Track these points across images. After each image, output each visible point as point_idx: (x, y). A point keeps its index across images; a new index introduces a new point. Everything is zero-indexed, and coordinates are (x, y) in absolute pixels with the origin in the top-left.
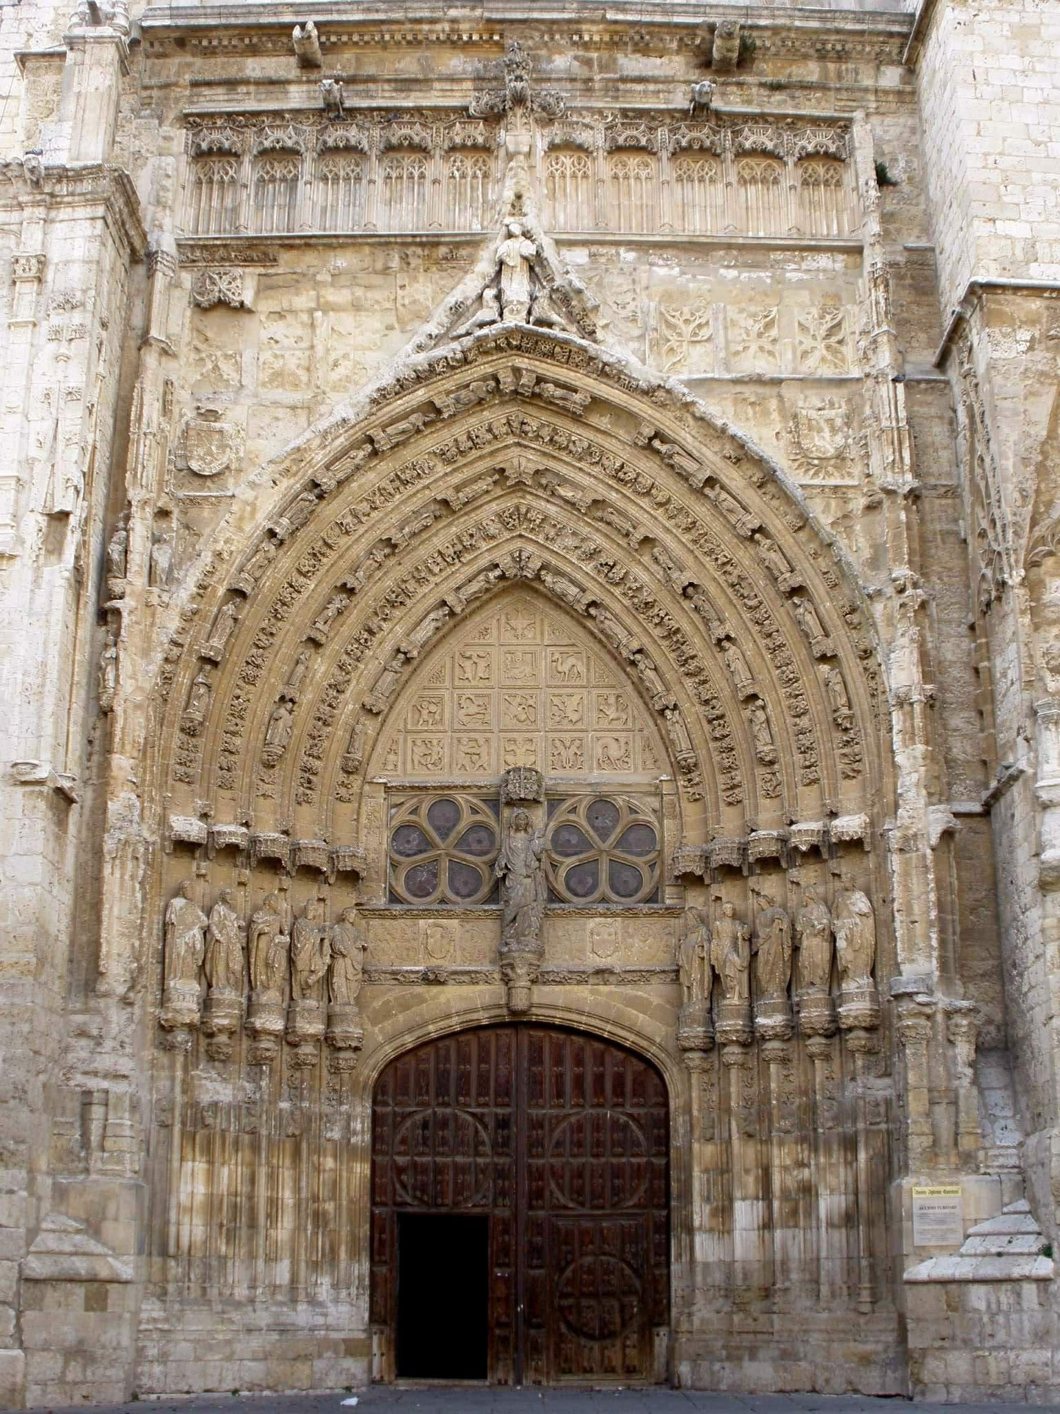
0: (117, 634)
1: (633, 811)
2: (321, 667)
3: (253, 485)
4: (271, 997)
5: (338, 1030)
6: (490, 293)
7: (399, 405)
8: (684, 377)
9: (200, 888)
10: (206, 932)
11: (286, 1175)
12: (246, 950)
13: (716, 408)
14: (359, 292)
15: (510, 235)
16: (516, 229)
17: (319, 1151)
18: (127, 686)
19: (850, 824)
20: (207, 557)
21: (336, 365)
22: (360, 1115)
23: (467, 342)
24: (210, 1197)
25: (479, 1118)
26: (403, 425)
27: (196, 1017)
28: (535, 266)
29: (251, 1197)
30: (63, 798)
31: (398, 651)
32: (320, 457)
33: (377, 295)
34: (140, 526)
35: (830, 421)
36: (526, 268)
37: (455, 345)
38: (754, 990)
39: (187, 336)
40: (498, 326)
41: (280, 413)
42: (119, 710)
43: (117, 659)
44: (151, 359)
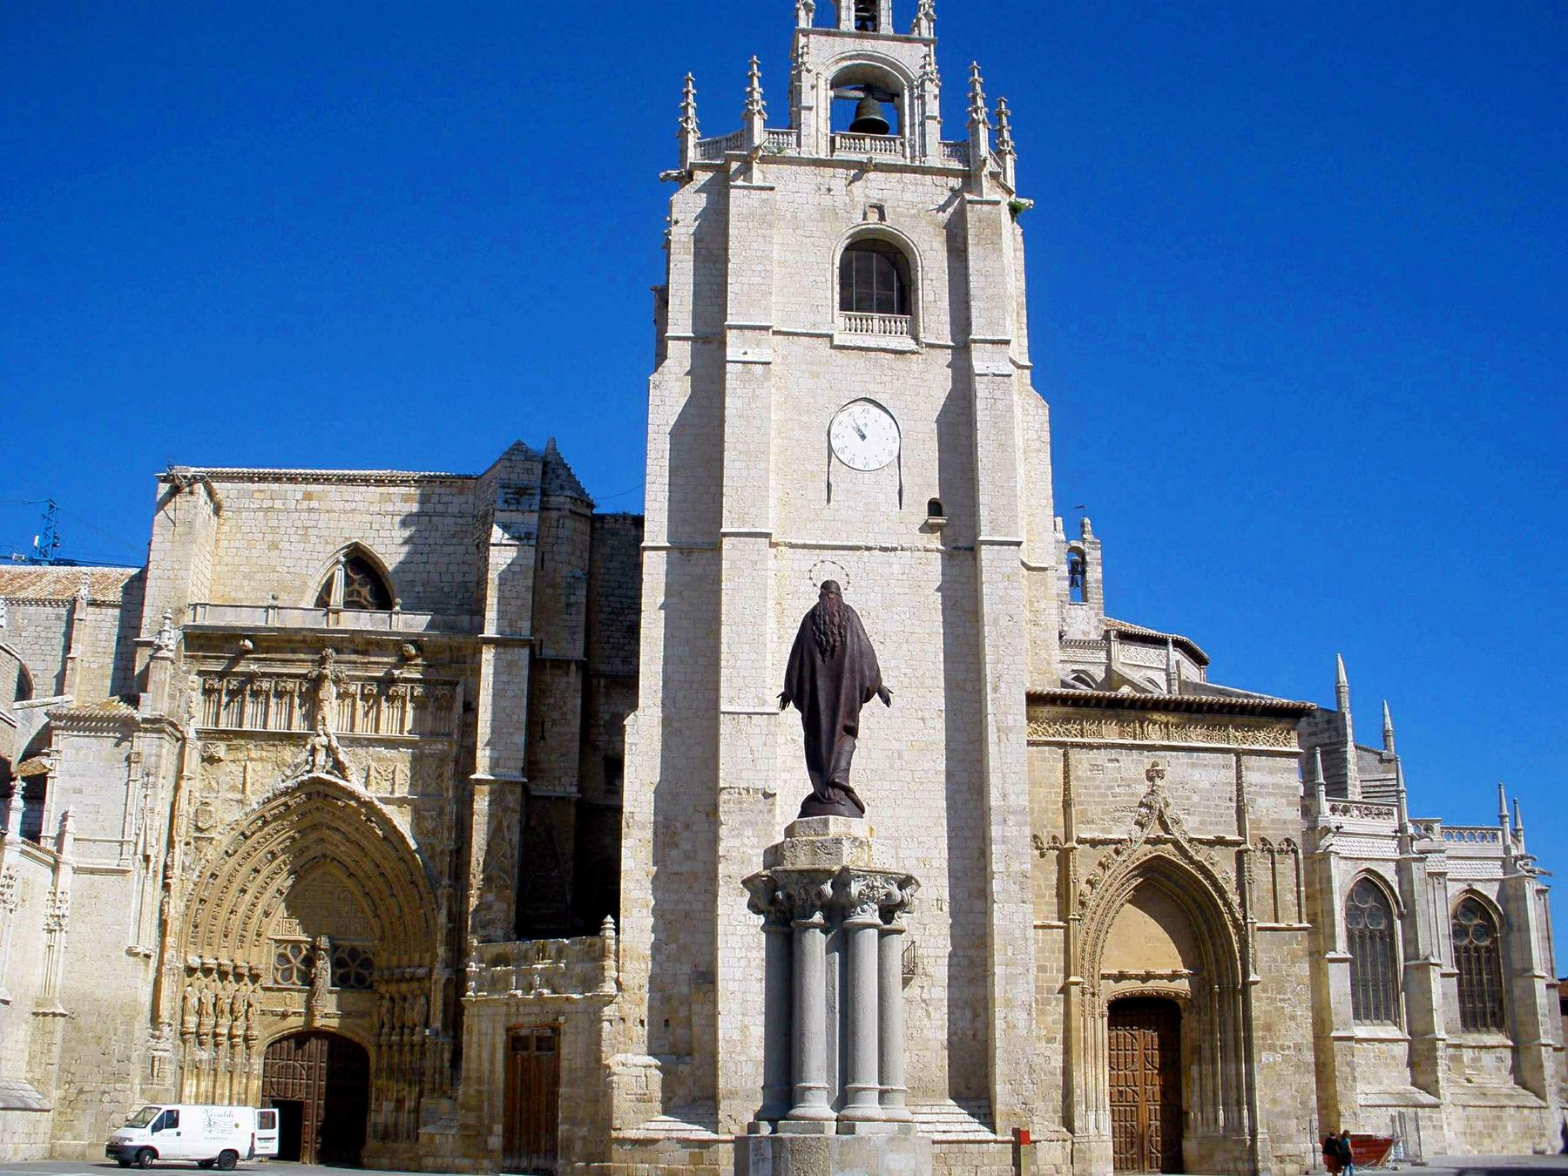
0: (168, 891)
1: (365, 952)
2: (248, 897)
3: (220, 833)
4: (225, 1021)
5: (249, 1033)
6: (311, 758)
7: (274, 804)
8: (379, 795)
9: (198, 982)
10: (200, 999)
11: (227, 1084)
12: (215, 1005)
13: (389, 811)
14: (264, 753)
15: (319, 736)
16: (321, 733)
17: (241, 1076)
18: (172, 911)
19: (421, 972)
20: (203, 862)
21: (253, 784)
22: (257, 1064)
23: (299, 779)
24: (197, 1092)
25: (302, 1066)
26: (276, 811)
27: (194, 1030)
28: (330, 750)
29: (214, 1093)
30: (148, 956)
31: (278, 890)
32: (245, 823)
33: (268, 754)
34: (179, 849)
35: (432, 817)
36: (324, 749)
37: (294, 781)
38: (393, 1028)
39: (199, 770)
40: (311, 775)
41: (232, 803)
42: (169, 921)
43: (168, 902)
44: (184, 783)
